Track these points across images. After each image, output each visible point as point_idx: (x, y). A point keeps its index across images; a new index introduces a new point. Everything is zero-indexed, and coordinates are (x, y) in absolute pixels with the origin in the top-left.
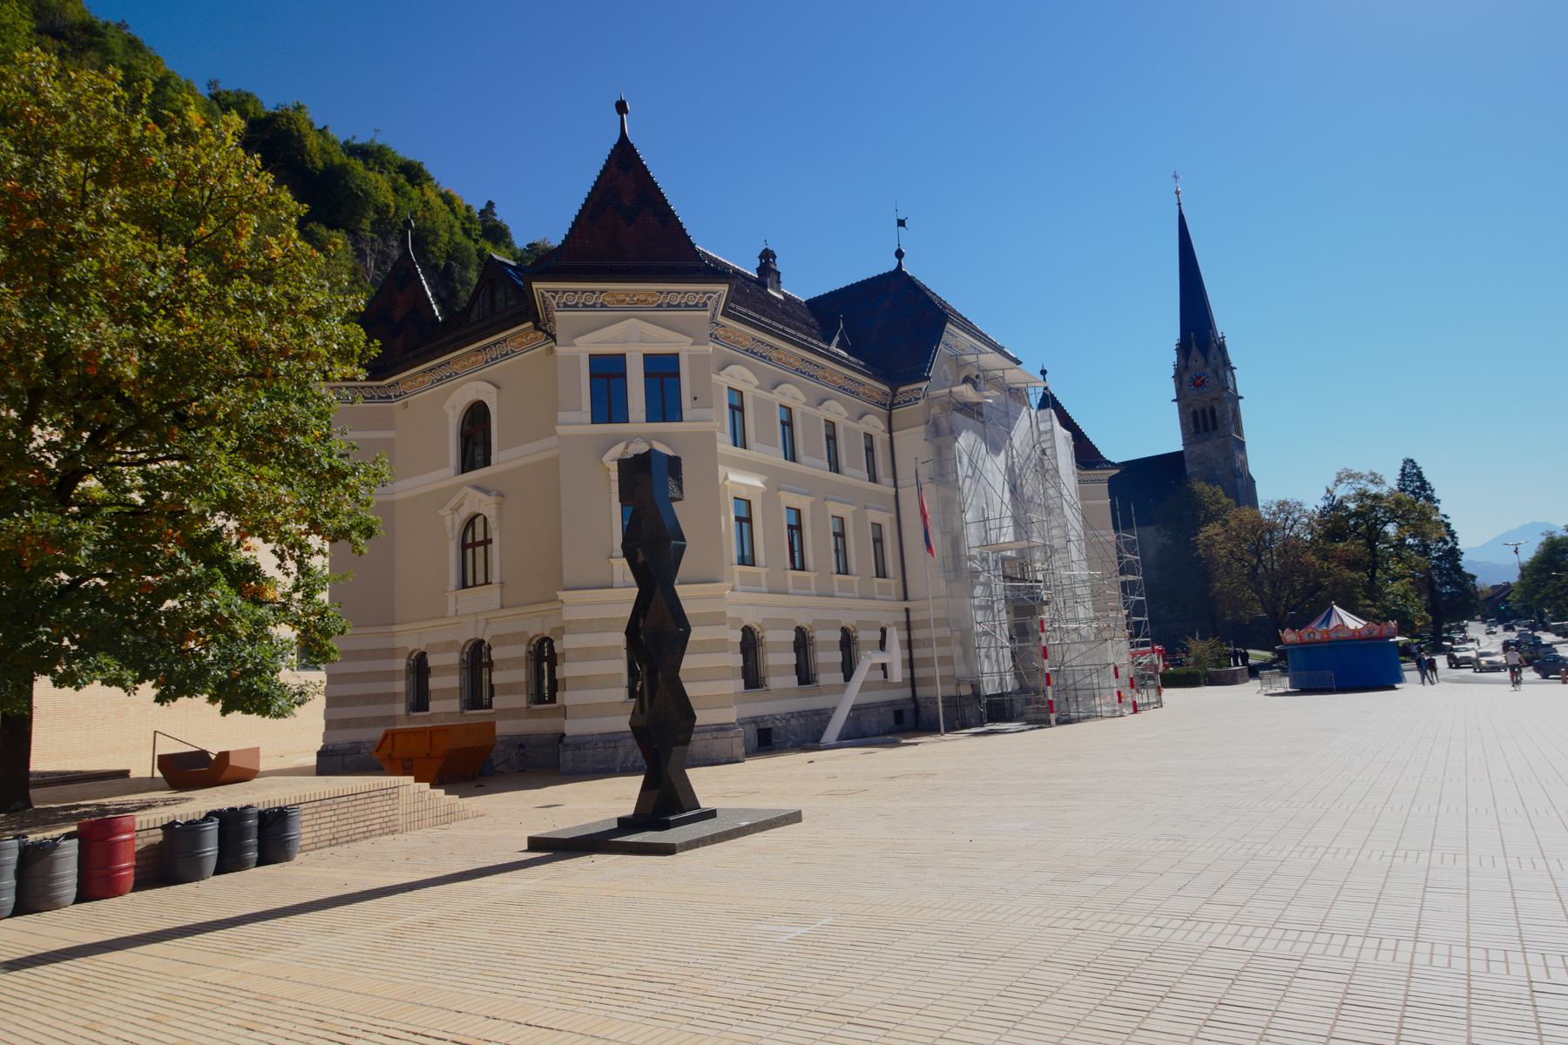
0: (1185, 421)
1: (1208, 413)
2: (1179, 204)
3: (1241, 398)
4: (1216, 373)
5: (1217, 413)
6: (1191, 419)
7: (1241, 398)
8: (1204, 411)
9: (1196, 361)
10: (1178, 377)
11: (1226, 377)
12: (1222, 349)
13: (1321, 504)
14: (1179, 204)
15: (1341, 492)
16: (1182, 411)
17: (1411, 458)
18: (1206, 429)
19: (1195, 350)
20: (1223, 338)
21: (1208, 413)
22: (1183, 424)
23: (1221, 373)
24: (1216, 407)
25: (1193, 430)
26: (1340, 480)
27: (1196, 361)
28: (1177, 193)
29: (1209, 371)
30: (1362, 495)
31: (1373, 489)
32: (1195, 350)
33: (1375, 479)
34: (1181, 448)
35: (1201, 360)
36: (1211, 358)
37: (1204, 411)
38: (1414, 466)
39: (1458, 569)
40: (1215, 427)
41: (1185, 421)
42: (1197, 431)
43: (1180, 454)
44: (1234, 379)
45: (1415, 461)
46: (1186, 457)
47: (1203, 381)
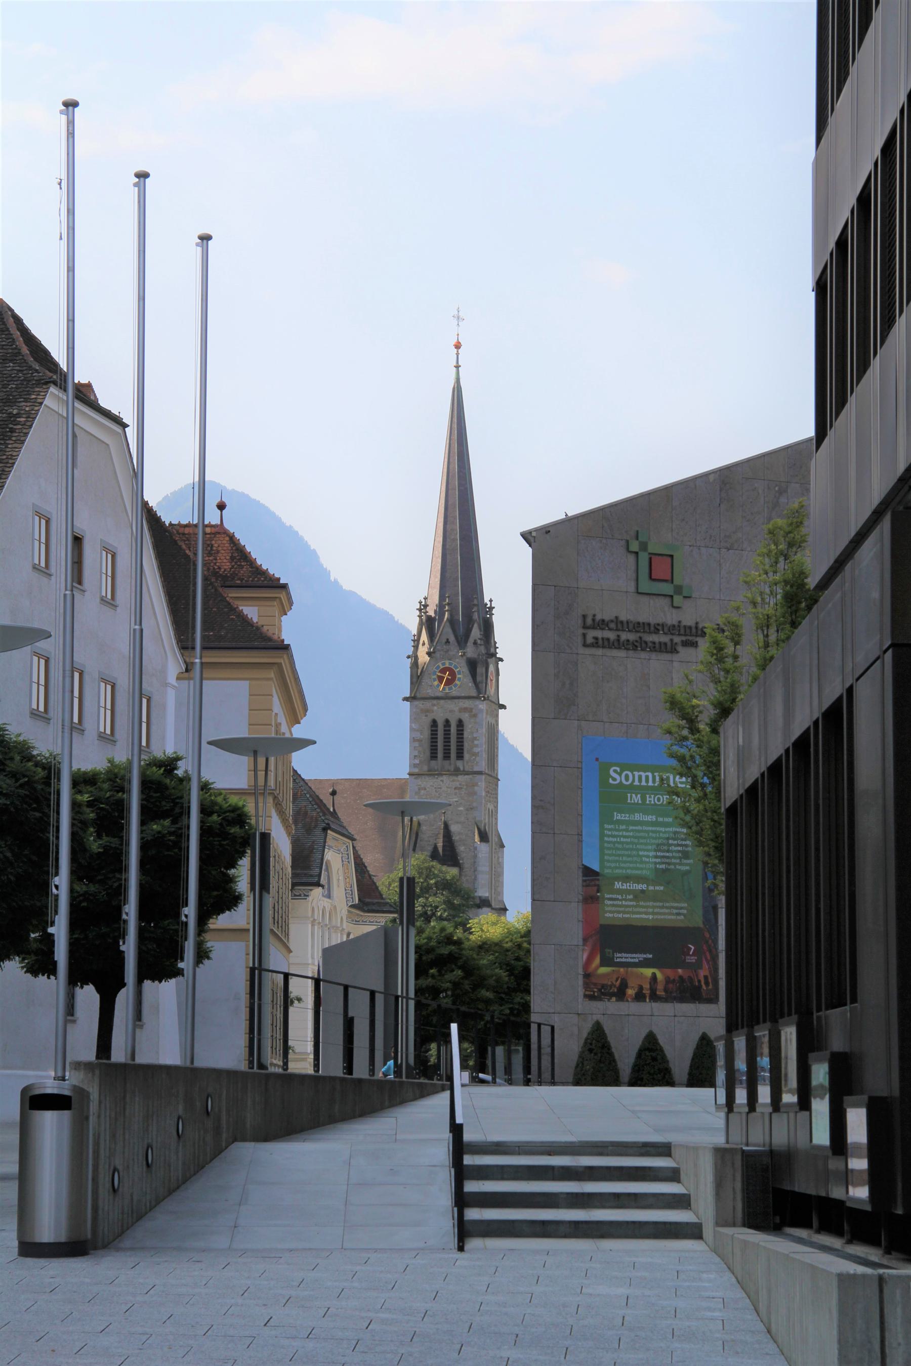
0: (418, 735)
2: (457, 367)
3: (503, 707)
6: (427, 733)
7: (503, 707)
8: (447, 723)
14: (457, 367)
16: (414, 718)
18: (447, 756)
20: (491, 608)
22: (413, 740)
25: (428, 753)
28: (458, 346)
37: (447, 723)
40: (460, 756)
41: (418, 735)
42: (433, 756)
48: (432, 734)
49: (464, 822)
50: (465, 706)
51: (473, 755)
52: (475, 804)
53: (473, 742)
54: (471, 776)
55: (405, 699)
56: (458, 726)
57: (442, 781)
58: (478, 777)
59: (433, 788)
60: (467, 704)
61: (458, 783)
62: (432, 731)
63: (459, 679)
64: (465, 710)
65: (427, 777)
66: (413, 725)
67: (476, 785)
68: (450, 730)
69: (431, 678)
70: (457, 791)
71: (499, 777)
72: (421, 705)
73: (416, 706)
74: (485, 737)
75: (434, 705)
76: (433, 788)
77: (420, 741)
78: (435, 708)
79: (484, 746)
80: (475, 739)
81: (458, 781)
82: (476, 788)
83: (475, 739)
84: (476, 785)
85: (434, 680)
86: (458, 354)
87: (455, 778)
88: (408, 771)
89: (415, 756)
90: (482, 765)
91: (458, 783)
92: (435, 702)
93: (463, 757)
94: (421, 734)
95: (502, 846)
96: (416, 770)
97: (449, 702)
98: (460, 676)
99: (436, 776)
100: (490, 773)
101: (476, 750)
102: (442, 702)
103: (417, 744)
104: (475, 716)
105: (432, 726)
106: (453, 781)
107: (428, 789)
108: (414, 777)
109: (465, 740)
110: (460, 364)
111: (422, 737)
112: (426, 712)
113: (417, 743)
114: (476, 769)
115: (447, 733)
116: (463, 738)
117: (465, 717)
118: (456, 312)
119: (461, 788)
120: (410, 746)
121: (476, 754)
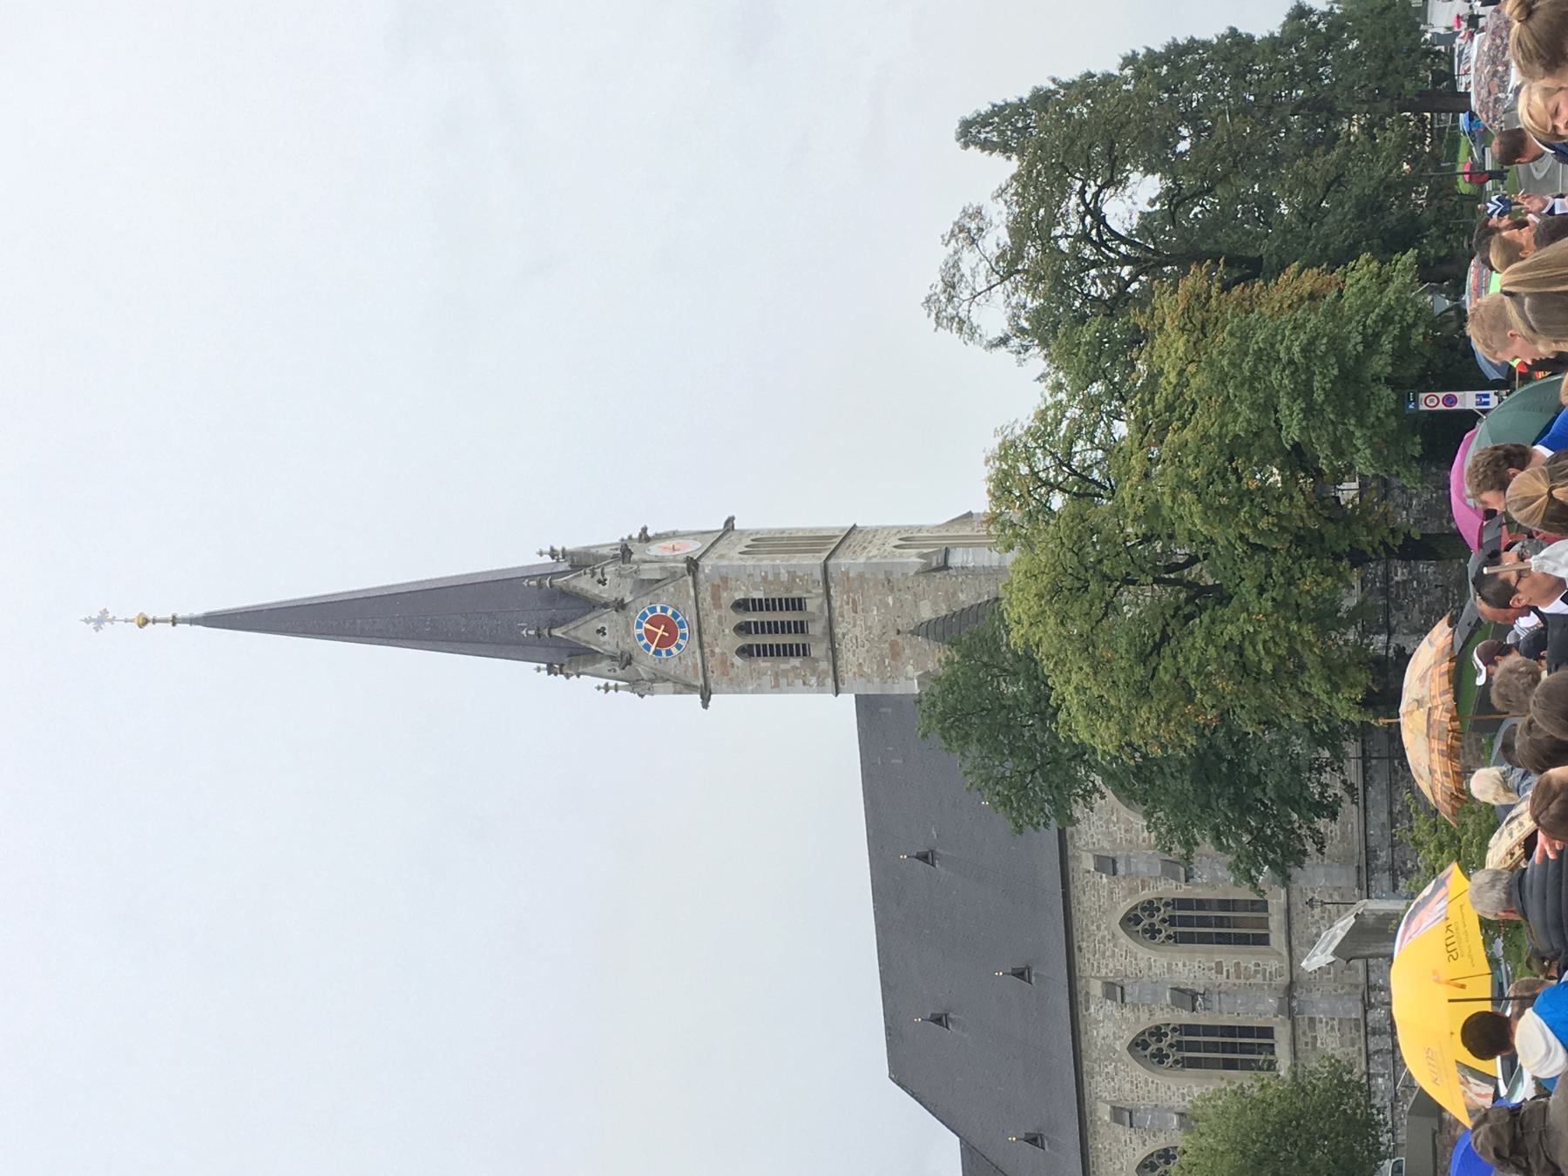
1: (752, 617)
2: (174, 621)
3: (730, 522)
4: (647, 586)
5: (758, 595)
6: (763, 664)
7: (730, 522)
8: (742, 629)
9: (606, 633)
10: (639, 686)
11: (659, 560)
12: (580, 561)
13: (1037, 361)
14: (174, 621)
15: (993, 316)
16: (737, 686)
17: (955, 126)
18: (800, 628)
19: (583, 631)
20: (553, 554)
21: (752, 617)
22: (776, 687)
23: (650, 572)
24: (739, 596)
25: (796, 662)
26: (961, 324)
27: (606, 633)
28: (146, 621)
29: (642, 606)
30: (1008, 265)
31: (997, 237)
32: (583, 631)
33: (968, 231)
34: (853, 695)
35: (608, 620)
36: (607, 593)
37: (742, 629)
38: (983, 121)
39: (1273, 44)
40: (797, 604)
41: (767, 680)
42: (802, 651)
43: (866, 706)
44: (674, 535)
45: (969, 115)
46: (872, 690)
47: (655, 622)
48: (765, 655)
49: (915, 594)
50: (709, 599)
51: (794, 581)
52: (881, 576)
53: (771, 583)
54: (832, 584)
55: (705, 706)
56: (747, 609)
57: (844, 635)
58: (831, 569)
59: (857, 651)
60: (706, 596)
61: (846, 607)
62: (759, 655)
63: (664, 610)
64: (716, 598)
65: (839, 663)
66: (750, 688)
67: (846, 573)
68: (756, 623)
69: (667, 660)
70: (859, 609)
71: (851, 525)
72: (715, 675)
73: (717, 683)
74: (761, 560)
75: (712, 651)
76: (857, 651)
77: (776, 675)
78: (717, 650)
79: (778, 562)
80: (765, 579)
81: (841, 607)
82: (852, 575)
83: (765, 579)
84: (846, 573)
85: (669, 653)
86: (154, 621)
87: (837, 611)
88: (832, 696)
89: (804, 683)
90: (812, 562)
91: (846, 607)
92: (707, 650)
93: (800, 600)
94: (765, 674)
95: (970, 515)
96: (829, 681)
97: (704, 626)
98: (658, 609)
99: (837, 646)
100: (833, 547)
101: (784, 577)
102: (706, 638)
103: (783, 681)
104: (725, 580)
105: (751, 655)
106: (843, 616)
107: (861, 661)
108: (840, 685)
109: (771, 596)
110: (169, 616)
111: (769, 673)
112: (723, 662)
113: (781, 681)
114: (818, 575)
115: (762, 628)
116: (767, 600)
117: (727, 597)
118: (92, 625)
119: (854, 600)
120: (787, 693)
121: (793, 576)
